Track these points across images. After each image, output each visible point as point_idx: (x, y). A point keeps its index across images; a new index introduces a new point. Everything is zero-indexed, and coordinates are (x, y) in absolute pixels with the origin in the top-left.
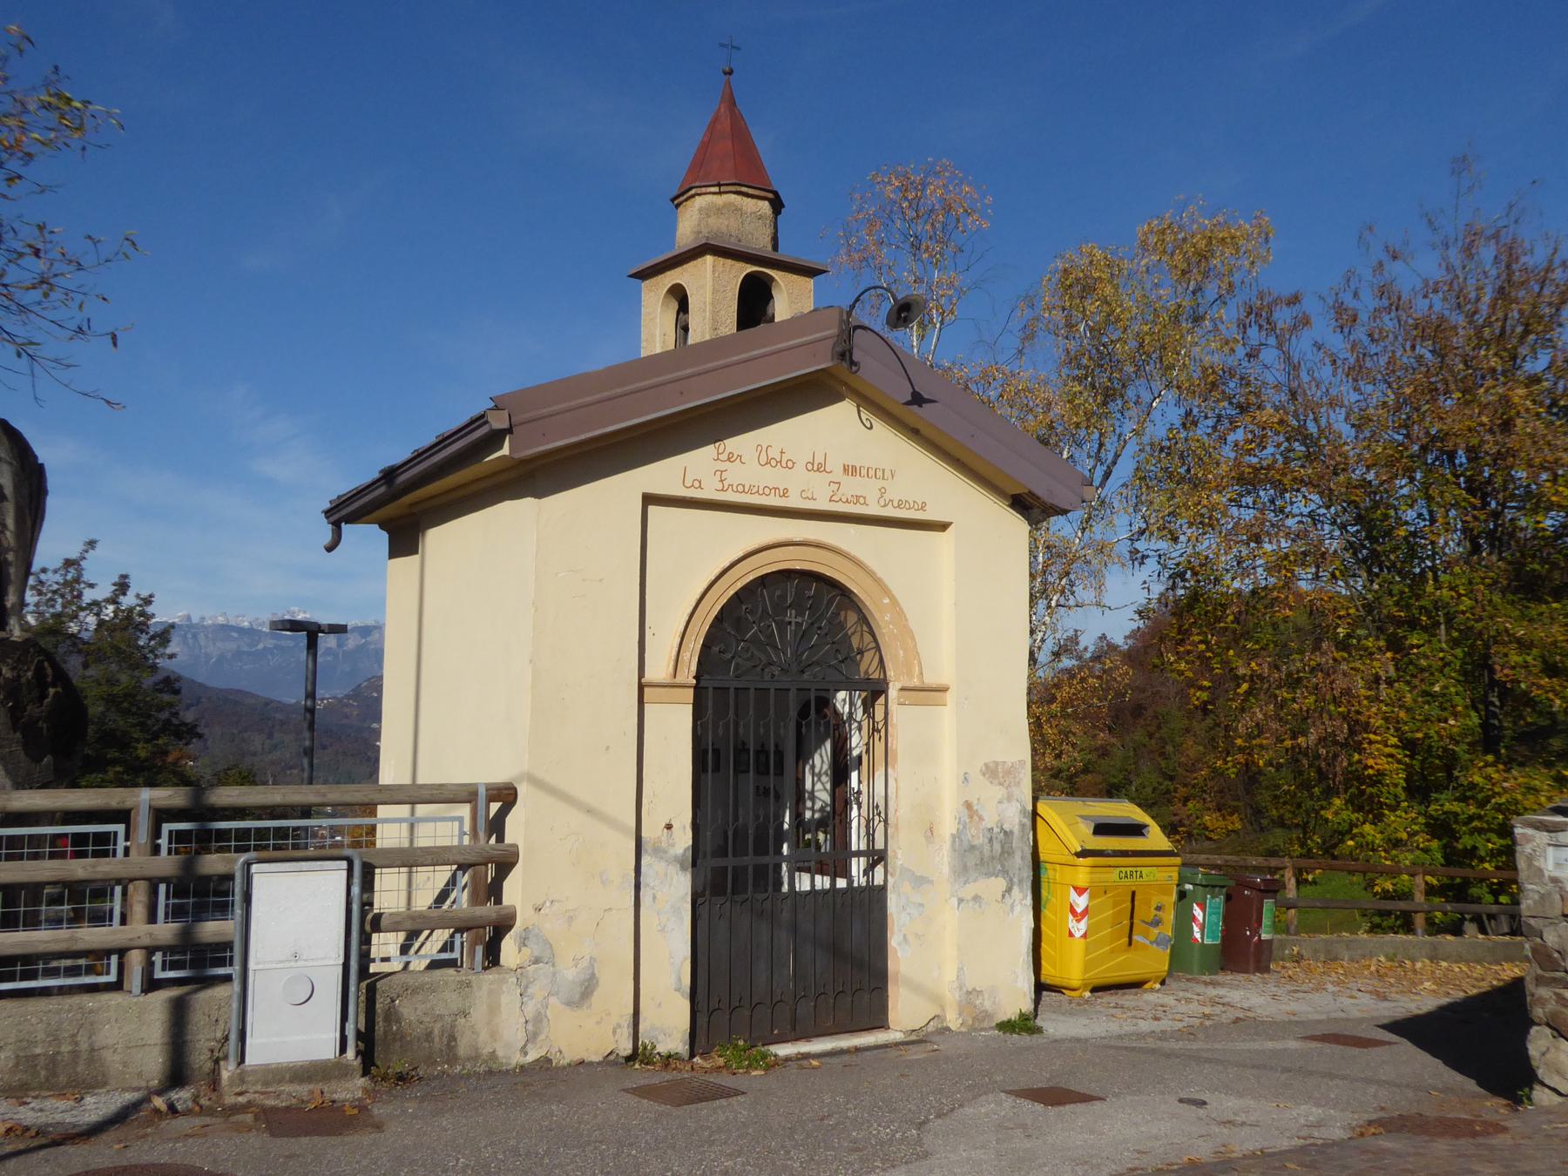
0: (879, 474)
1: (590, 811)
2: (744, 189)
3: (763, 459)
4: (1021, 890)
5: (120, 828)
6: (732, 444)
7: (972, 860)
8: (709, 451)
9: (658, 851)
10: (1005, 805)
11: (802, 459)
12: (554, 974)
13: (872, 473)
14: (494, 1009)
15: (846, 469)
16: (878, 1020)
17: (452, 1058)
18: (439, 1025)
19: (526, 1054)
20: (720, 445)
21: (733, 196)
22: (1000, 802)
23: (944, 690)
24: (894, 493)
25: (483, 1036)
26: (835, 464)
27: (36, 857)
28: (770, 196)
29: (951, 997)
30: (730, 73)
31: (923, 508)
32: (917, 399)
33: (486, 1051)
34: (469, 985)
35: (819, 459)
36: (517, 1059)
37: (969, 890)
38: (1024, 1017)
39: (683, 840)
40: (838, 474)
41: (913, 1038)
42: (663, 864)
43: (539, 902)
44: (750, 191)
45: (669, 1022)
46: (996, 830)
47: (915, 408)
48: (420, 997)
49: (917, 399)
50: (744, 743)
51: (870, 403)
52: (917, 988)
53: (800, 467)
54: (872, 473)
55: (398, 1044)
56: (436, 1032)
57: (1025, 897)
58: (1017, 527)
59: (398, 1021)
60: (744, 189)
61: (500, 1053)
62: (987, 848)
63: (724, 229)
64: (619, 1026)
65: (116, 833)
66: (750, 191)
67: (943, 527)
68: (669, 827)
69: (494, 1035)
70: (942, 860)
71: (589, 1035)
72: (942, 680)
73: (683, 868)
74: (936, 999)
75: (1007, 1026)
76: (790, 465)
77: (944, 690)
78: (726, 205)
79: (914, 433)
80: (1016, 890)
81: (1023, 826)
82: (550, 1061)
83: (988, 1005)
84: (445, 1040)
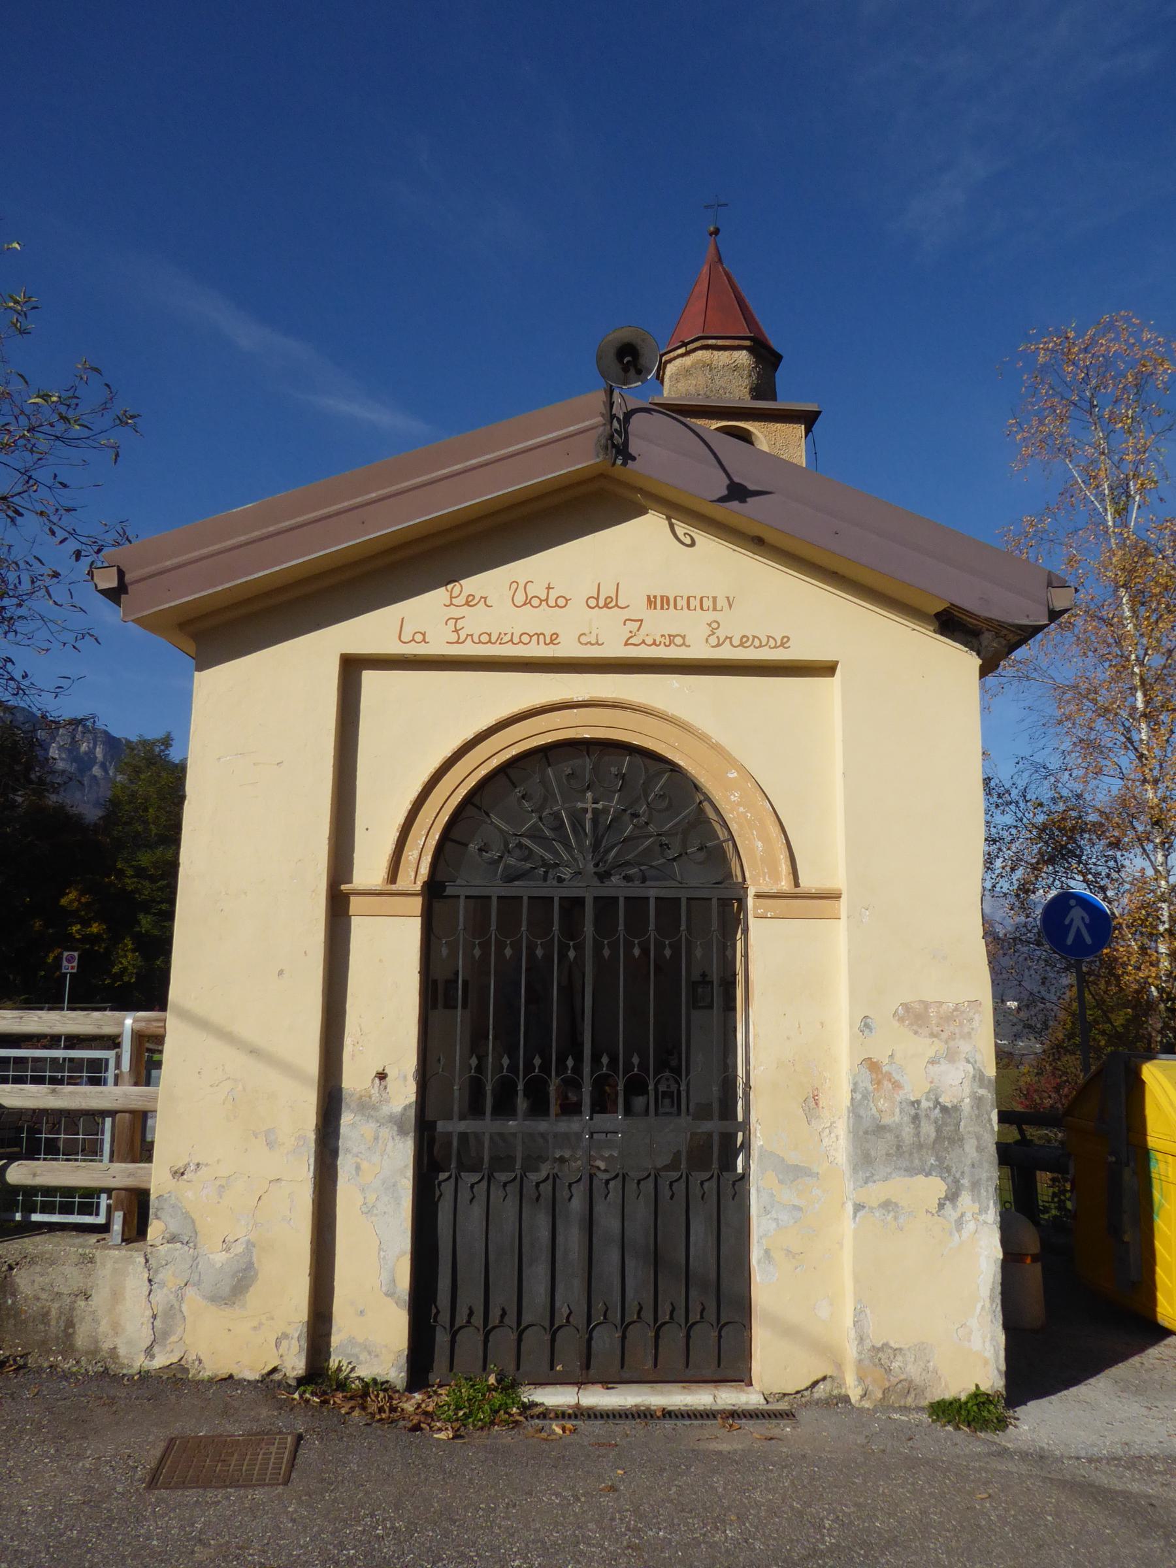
0: (707, 603)
1: (254, 1052)
2: (711, 342)
3: (520, 598)
4: (976, 1197)
5: (110, 1055)
6: (471, 584)
7: (880, 1147)
8: (440, 595)
9: (366, 1107)
10: (944, 1066)
11: (581, 590)
12: (195, 1258)
13: (694, 603)
14: (116, 1296)
15: (651, 602)
16: (732, 1365)
17: (68, 1348)
18: (56, 1305)
19: (153, 1357)
20: (455, 587)
21: (700, 353)
22: (933, 1062)
23: (836, 896)
24: (734, 624)
25: (104, 1327)
26: (634, 598)
27: (72, 1081)
28: (747, 343)
29: (851, 1352)
30: (716, 232)
31: (784, 642)
32: (737, 492)
33: (106, 1346)
34: (92, 1260)
35: (607, 591)
36: (139, 1362)
37: (877, 1192)
38: (980, 1399)
39: (403, 1093)
40: (639, 608)
41: (783, 1406)
42: (373, 1125)
43: (180, 1164)
44: (720, 342)
45: (374, 1335)
46: (925, 1104)
47: (735, 505)
48: (38, 1269)
49: (737, 492)
50: (704, 975)
51: (676, 510)
52: (789, 1331)
53: (578, 602)
54: (694, 603)
55: (12, 1321)
56: (54, 1312)
57: (983, 1210)
58: (962, 662)
59: (14, 1295)
60: (711, 342)
61: (122, 1351)
62: (907, 1131)
63: (692, 390)
64: (285, 1336)
65: (107, 1060)
66: (720, 342)
67: (827, 669)
68: (382, 1076)
69: (116, 1328)
70: (839, 1145)
71: (256, 1339)
72: (838, 880)
73: (402, 1132)
74: (824, 1349)
75: (947, 1411)
76: (563, 602)
77: (836, 896)
78: (694, 365)
79: (757, 543)
80: (965, 1199)
81: (978, 1101)
82: (186, 1371)
83: (913, 1371)
84: (62, 1324)
